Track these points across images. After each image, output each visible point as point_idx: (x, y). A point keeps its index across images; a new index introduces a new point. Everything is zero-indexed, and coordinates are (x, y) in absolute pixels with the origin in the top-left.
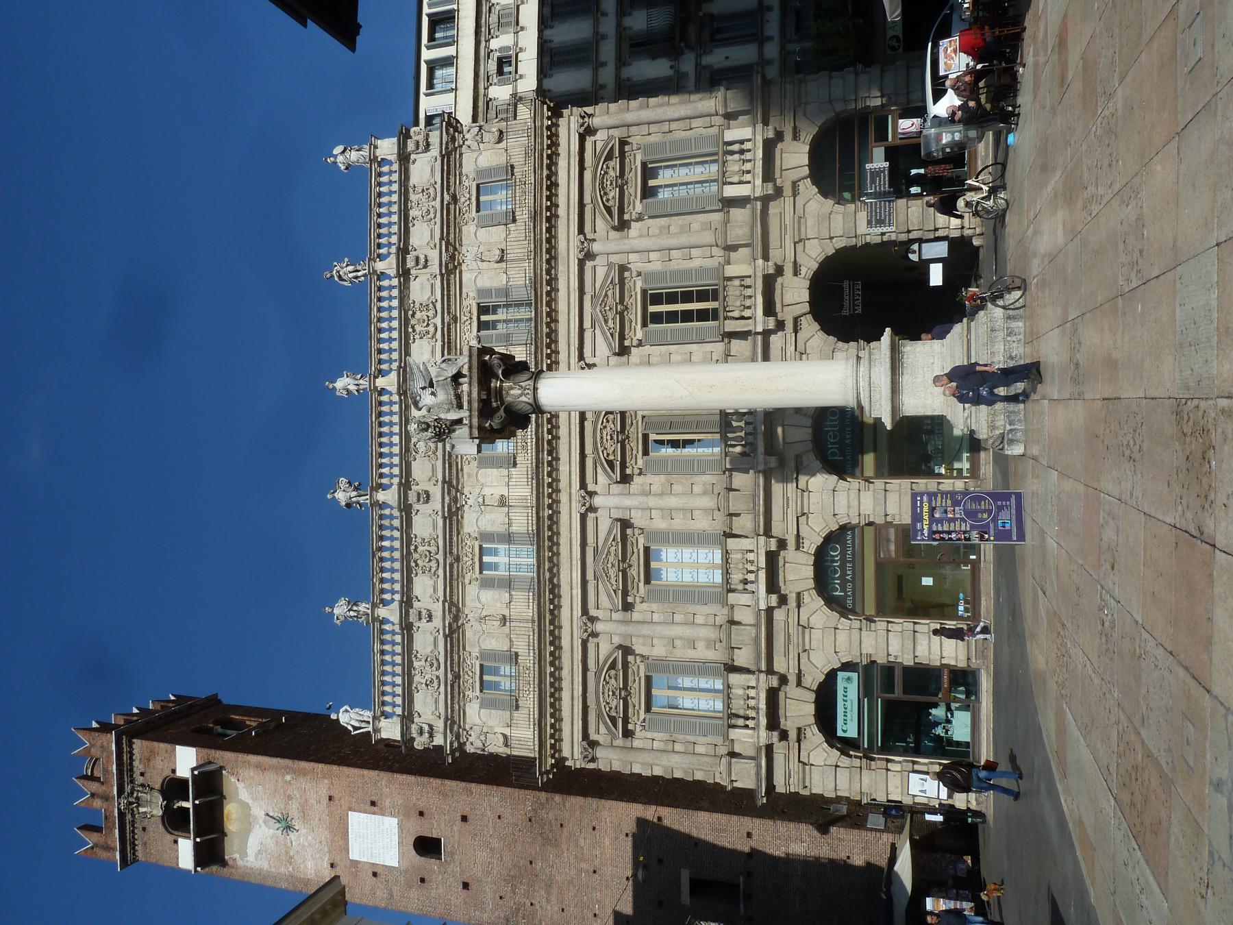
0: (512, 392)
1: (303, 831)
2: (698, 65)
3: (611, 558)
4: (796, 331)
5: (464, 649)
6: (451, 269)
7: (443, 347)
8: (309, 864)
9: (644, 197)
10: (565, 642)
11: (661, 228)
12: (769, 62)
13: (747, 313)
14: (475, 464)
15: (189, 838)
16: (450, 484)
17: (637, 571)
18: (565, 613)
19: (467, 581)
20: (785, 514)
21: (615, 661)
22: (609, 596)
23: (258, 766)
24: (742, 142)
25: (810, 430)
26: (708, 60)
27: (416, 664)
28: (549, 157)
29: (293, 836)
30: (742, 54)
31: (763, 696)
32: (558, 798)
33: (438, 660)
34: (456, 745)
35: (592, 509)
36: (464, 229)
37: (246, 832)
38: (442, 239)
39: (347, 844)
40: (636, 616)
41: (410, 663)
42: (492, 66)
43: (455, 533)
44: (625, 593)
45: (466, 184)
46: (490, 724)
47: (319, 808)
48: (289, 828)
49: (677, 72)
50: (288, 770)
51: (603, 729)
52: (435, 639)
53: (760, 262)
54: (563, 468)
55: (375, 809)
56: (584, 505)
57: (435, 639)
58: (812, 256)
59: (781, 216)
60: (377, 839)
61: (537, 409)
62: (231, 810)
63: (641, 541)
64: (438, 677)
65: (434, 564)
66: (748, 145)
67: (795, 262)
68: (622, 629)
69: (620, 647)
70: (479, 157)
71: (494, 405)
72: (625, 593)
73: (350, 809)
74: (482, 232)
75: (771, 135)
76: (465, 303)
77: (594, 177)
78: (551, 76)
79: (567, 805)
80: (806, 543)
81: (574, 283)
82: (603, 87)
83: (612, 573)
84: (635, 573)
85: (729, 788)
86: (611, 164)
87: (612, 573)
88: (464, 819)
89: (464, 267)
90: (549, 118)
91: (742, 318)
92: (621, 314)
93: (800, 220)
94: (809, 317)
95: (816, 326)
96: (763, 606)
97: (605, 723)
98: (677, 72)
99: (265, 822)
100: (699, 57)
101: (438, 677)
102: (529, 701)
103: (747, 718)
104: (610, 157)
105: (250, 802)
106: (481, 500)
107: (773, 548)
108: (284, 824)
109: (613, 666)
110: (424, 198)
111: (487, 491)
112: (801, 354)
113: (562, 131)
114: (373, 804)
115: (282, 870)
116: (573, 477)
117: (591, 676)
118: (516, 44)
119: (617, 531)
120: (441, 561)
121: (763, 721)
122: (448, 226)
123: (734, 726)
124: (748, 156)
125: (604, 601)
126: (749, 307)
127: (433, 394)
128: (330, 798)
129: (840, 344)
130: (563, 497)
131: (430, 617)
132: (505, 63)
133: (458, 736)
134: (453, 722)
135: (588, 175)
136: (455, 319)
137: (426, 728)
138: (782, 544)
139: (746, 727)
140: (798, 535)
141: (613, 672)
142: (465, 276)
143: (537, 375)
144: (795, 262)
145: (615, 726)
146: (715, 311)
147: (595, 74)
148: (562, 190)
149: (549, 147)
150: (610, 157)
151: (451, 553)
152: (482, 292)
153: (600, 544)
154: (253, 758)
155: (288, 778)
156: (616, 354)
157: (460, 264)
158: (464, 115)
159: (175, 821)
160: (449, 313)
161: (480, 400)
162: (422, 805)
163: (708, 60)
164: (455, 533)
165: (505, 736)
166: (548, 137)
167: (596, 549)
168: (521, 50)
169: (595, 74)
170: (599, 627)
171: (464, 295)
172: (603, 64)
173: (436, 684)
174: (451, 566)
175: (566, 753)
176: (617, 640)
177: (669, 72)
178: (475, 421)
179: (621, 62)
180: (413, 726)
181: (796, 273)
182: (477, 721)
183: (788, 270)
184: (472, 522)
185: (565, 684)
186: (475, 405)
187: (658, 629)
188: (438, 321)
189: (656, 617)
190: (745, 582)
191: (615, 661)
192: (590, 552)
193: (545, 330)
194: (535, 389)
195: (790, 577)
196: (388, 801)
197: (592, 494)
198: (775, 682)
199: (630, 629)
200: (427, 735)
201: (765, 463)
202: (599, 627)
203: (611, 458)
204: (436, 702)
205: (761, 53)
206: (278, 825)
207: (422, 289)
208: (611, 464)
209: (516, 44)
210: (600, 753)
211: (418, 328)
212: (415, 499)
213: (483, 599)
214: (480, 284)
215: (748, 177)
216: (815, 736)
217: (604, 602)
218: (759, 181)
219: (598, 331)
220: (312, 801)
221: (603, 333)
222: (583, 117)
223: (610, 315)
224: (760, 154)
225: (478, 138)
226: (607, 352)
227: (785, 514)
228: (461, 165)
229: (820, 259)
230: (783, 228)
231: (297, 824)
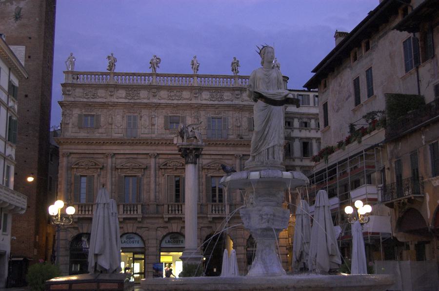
0: (191, 157)
1: (16, 25)
3: (133, 164)
4: (208, 227)
5: (99, 109)
7: (207, 104)
10: (104, 147)
13: (214, 212)
14: (166, 115)
16: (159, 105)
17: (129, 173)
18: (115, 147)
19: (124, 110)
21: (98, 165)
25: (176, 231)
27: (93, 89)
29: (13, 20)
31: (90, 216)
32: (37, 134)
33: (95, 98)
34: (65, 105)
35: (151, 157)
36: (247, 113)
38: (244, 105)
40: (114, 172)
41: (94, 87)
42: (305, 120)
43: (142, 106)
44: (121, 169)
46: (73, 118)
51: (74, 160)
52: (103, 97)
54: (164, 148)
55: (27, 58)
57: (103, 97)
61: (187, 163)
63: (140, 175)
64: (89, 98)
65: (130, 98)
68: (109, 167)
69: (103, 166)
71: (188, 151)
73: (26, 47)
74: (245, 119)
78: (299, 142)
79: (35, 138)
80: (139, 230)
81: (227, 153)
82: (294, 160)
83: (129, 165)
84: (128, 172)
87: (129, 165)
88: (26, 96)
89: (234, 112)
91: (212, 210)
92: (216, 169)
101: (89, 98)
102: (83, 134)
103: (82, 211)
106: (153, 117)
107: (138, 220)
108: (18, 17)
109: (96, 164)
111: (156, 119)
112: (200, 229)
114: (29, 57)
116: (161, 151)
117: (92, 156)
119: (143, 166)
120: (131, 101)
121: (81, 216)
122: (249, 107)
123: (79, 207)
125: (119, 161)
127: (191, 131)
128: (30, 38)
130: (154, 148)
131: (111, 96)
132: (305, 125)
133: (68, 105)
134: (73, 104)
136: (217, 108)
137: (70, 93)
138: (140, 222)
140: (142, 227)
142: (231, 112)
143: (195, 163)
145: (76, 165)
146: (215, 201)
147: (298, 158)
151: (135, 105)
152: (225, 119)
153: (138, 160)
155: (37, 19)
156: (202, 167)
160: (219, 107)
161: (189, 148)
164: (142, 106)
165: (68, 124)
169: (298, 158)
170: (110, 160)
173: (87, 97)
174: (130, 105)
175: (65, 147)
176: (105, 165)
178: (183, 147)
180: (71, 88)
182: (74, 113)
184: (145, 112)
186: (188, 147)
187: (110, 180)
188: (216, 102)
189: (114, 179)
190: (127, 211)
191: (98, 165)
192: (135, 156)
193: (211, 143)
194: (192, 163)
197: (155, 157)
199: (109, 171)
200: (68, 93)
201: (166, 218)
202: (110, 160)
203: (168, 165)
204: (80, 97)
206: (17, 13)
207: (227, 96)
208: (166, 165)
209: (312, 129)
210: (65, 159)
212: (154, 91)
213: (118, 116)
214: (229, 118)
217: (119, 162)
223: (216, 165)
226: (204, 163)
231: (18, 22)
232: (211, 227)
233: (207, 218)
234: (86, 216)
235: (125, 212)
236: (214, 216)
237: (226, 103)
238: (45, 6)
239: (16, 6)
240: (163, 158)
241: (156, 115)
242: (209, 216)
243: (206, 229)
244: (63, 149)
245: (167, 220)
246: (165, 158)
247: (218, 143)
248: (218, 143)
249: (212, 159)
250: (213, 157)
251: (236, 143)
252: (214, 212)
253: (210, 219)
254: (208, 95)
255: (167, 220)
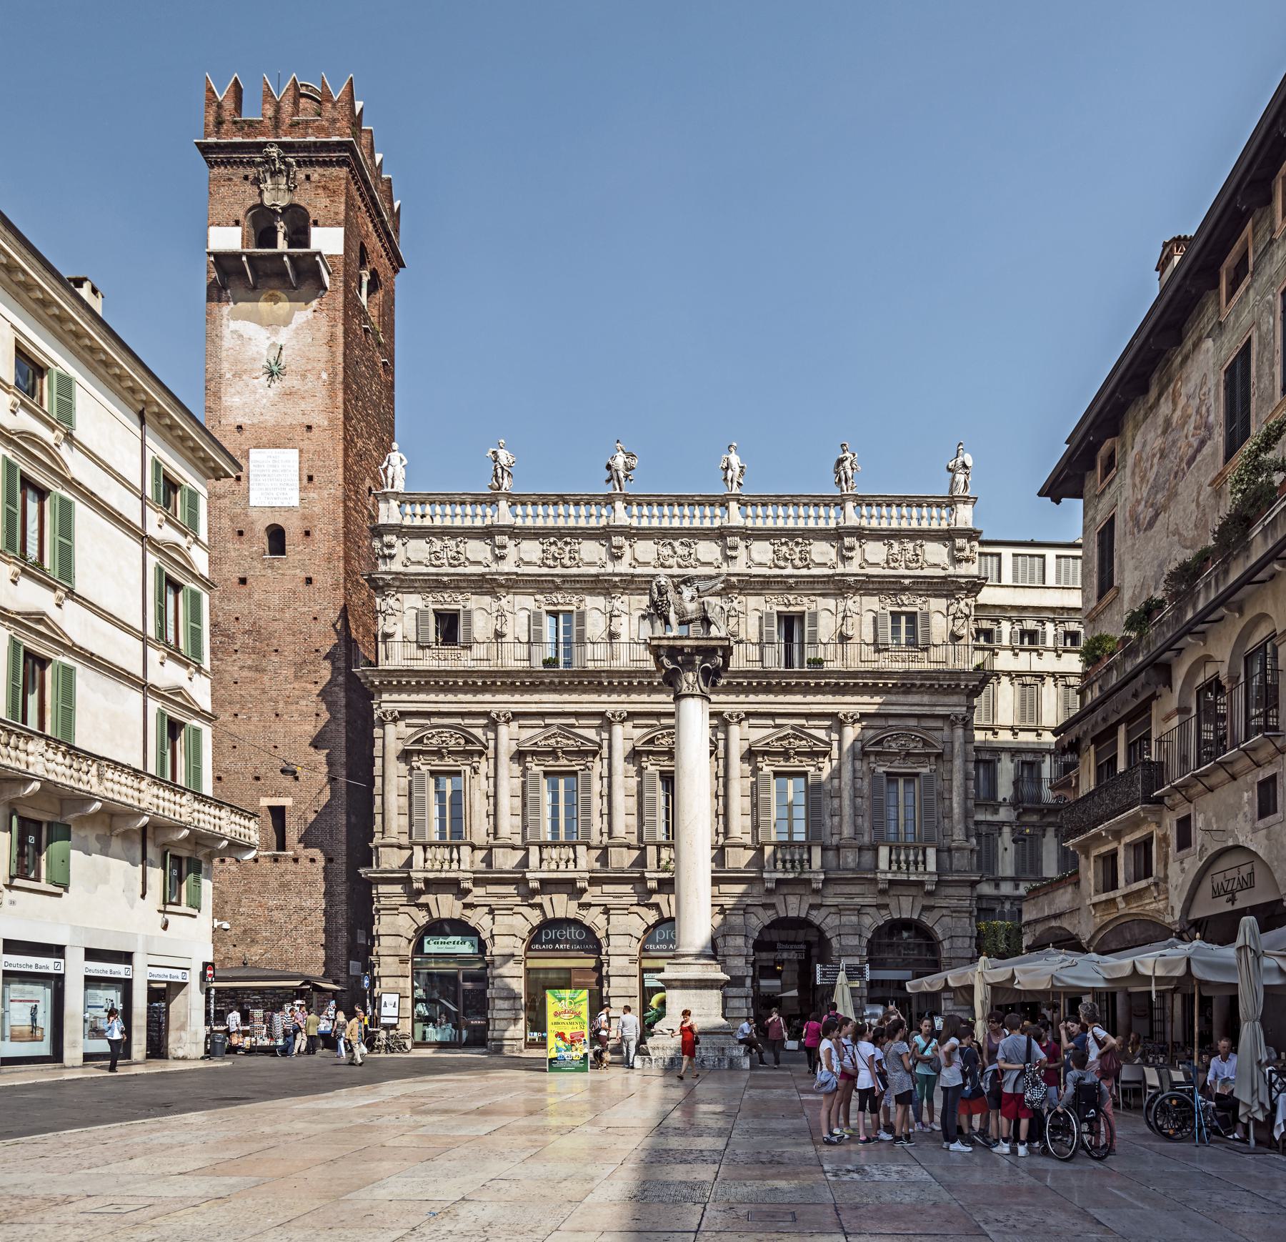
2: (1003, 823)
3: (565, 741)
4: (765, 906)
6: (838, 587)
8: (236, 399)
9: (888, 774)
11: (860, 790)
12: (997, 886)
15: (245, 242)
20: (608, 895)
22: (531, 738)
23: (332, 337)
24: (924, 862)
26: (1006, 830)
28: (932, 685)
29: (264, 379)
30: (1007, 864)
37: (260, 321)
39: (264, 447)
45: (918, 601)
47: (296, 414)
48: (272, 374)
49: (1000, 804)
50: (333, 375)
53: (822, 877)
56: (614, 716)
58: (826, 921)
59: (862, 895)
60: (274, 482)
62: (284, 306)
66: (921, 868)
67: (822, 905)
70: (939, 617)
72: (534, 753)
75: (928, 887)
76: (805, 599)
77: (908, 729)
85: (371, 845)
86: (920, 745)
90: (966, 686)
93: (859, 910)
94: (775, 917)
95: (767, 922)
96: (528, 875)
97: (416, 733)
98: (1000, 804)
99: (274, 344)
100: (1009, 824)
104: (926, 743)
105: (293, 326)
108: (275, 369)
110: (909, 556)
113: (954, 699)
115: (225, 366)
118: (1047, 650)
121: (431, 875)
124: (912, 868)
126: (784, 866)
129: (751, 941)
135: (912, 723)
139: (425, 861)
141: (462, 741)
144: (822, 905)
148: (901, 699)
149: (941, 686)
150: (926, 743)
154: (340, 330)
157: (842, 594)
158: (988, 596)
159: (261, 224)
162: (316, 534)
163: (1006, 830)
166: (949, 686)
167: (573, 726)
168: (1040, 655)
171: (813, 598)
172: (1015, 734)
177: (1000, 799)
179: (1015, 751)
181: (812, 907)
183: (817, 900)
185: (450, 697)
192: (572, 721)
195: (555, 897)
196: (315, 496)
198: (465, 885)
205: (1005, 879)
206: (273, 362)
211: (784, 549)
215: (894, 867)
216: (422, 918)
217: (528, 735)
218: (889, 876)
219: (771, 731)
220: (303, 406)
221: (768, 736)
222: (964, 719)
223: (785, 743)
224: (913, 878)
225: (959, 614)
226: (752, 739)
227: (608, 895)
228: (936, 596)
229: (823, 926)
230: (850, 896)
232: (772, 906)
233: (763, 880)
234: (443, 875)
235: (545, 863)
236: (780, 876)
237: (815, 571)
238: (341, 340)
239: (268, 343)
240: (647, 726)
241: (626, 610)
242: (765, 875)
243: (760, 911)
244: (388, 703)
245: (652, 885)
246: (647, 726)
247: (793, 682)
248: (793, 682)
249: (776, 726)
250: (778, 721)
251: (842, 682)
252: (780, 865)
253: (769, 885)
254: (766, 552)
255: (652, 885)
